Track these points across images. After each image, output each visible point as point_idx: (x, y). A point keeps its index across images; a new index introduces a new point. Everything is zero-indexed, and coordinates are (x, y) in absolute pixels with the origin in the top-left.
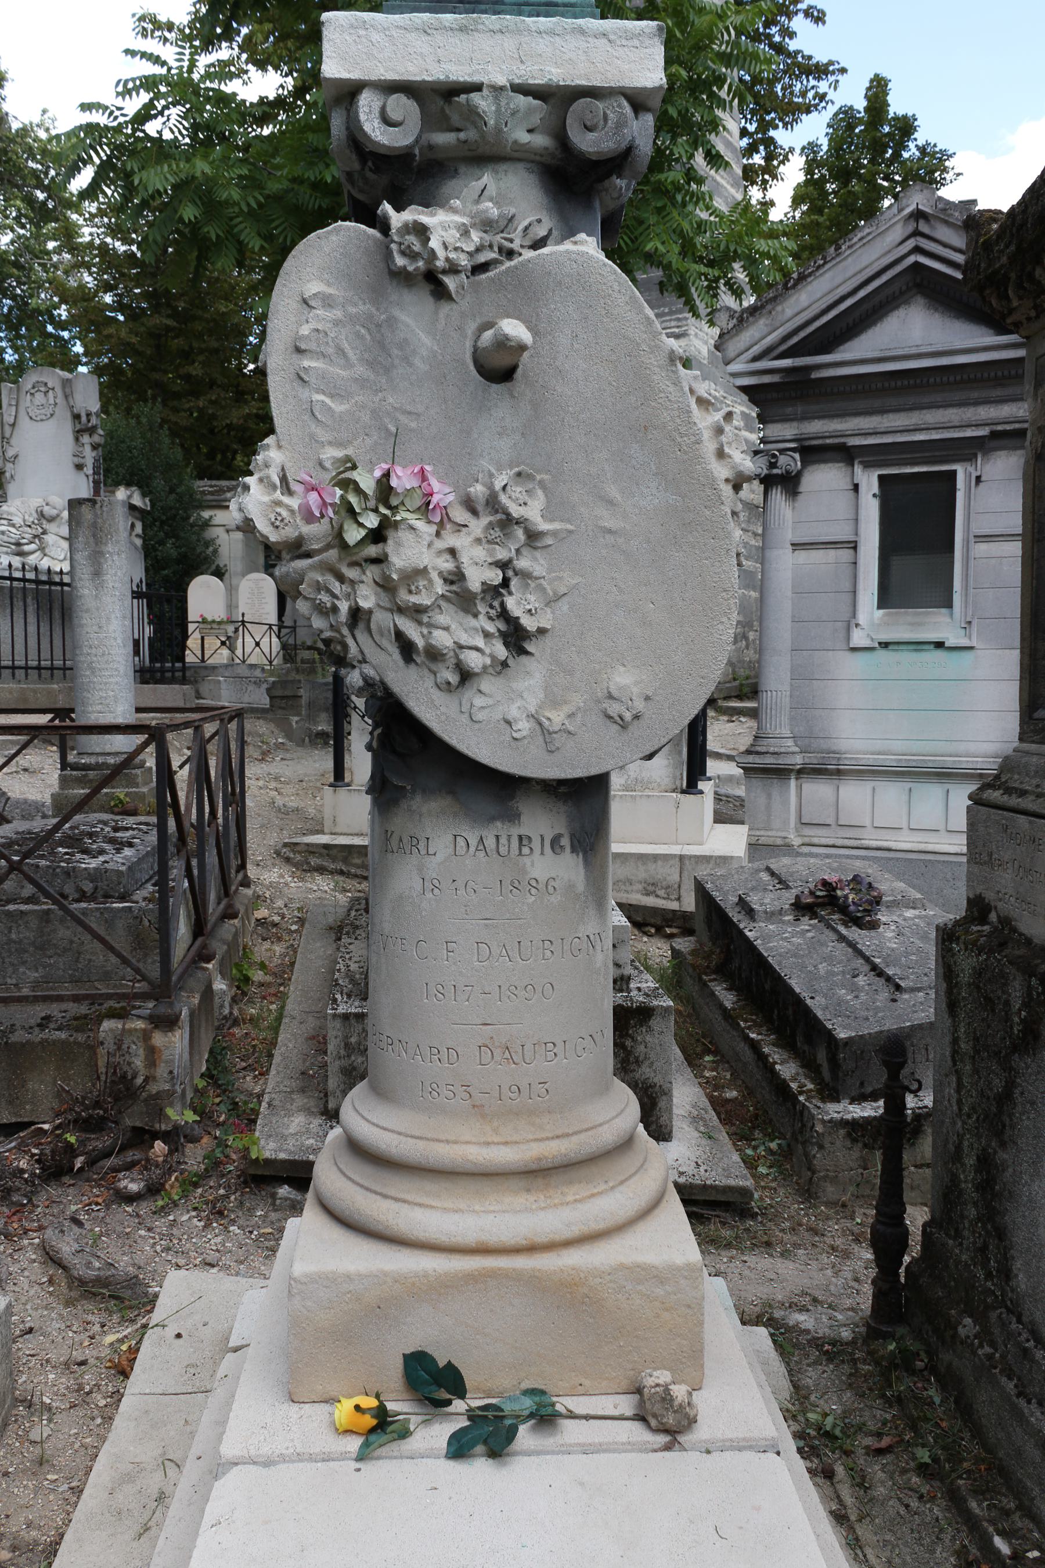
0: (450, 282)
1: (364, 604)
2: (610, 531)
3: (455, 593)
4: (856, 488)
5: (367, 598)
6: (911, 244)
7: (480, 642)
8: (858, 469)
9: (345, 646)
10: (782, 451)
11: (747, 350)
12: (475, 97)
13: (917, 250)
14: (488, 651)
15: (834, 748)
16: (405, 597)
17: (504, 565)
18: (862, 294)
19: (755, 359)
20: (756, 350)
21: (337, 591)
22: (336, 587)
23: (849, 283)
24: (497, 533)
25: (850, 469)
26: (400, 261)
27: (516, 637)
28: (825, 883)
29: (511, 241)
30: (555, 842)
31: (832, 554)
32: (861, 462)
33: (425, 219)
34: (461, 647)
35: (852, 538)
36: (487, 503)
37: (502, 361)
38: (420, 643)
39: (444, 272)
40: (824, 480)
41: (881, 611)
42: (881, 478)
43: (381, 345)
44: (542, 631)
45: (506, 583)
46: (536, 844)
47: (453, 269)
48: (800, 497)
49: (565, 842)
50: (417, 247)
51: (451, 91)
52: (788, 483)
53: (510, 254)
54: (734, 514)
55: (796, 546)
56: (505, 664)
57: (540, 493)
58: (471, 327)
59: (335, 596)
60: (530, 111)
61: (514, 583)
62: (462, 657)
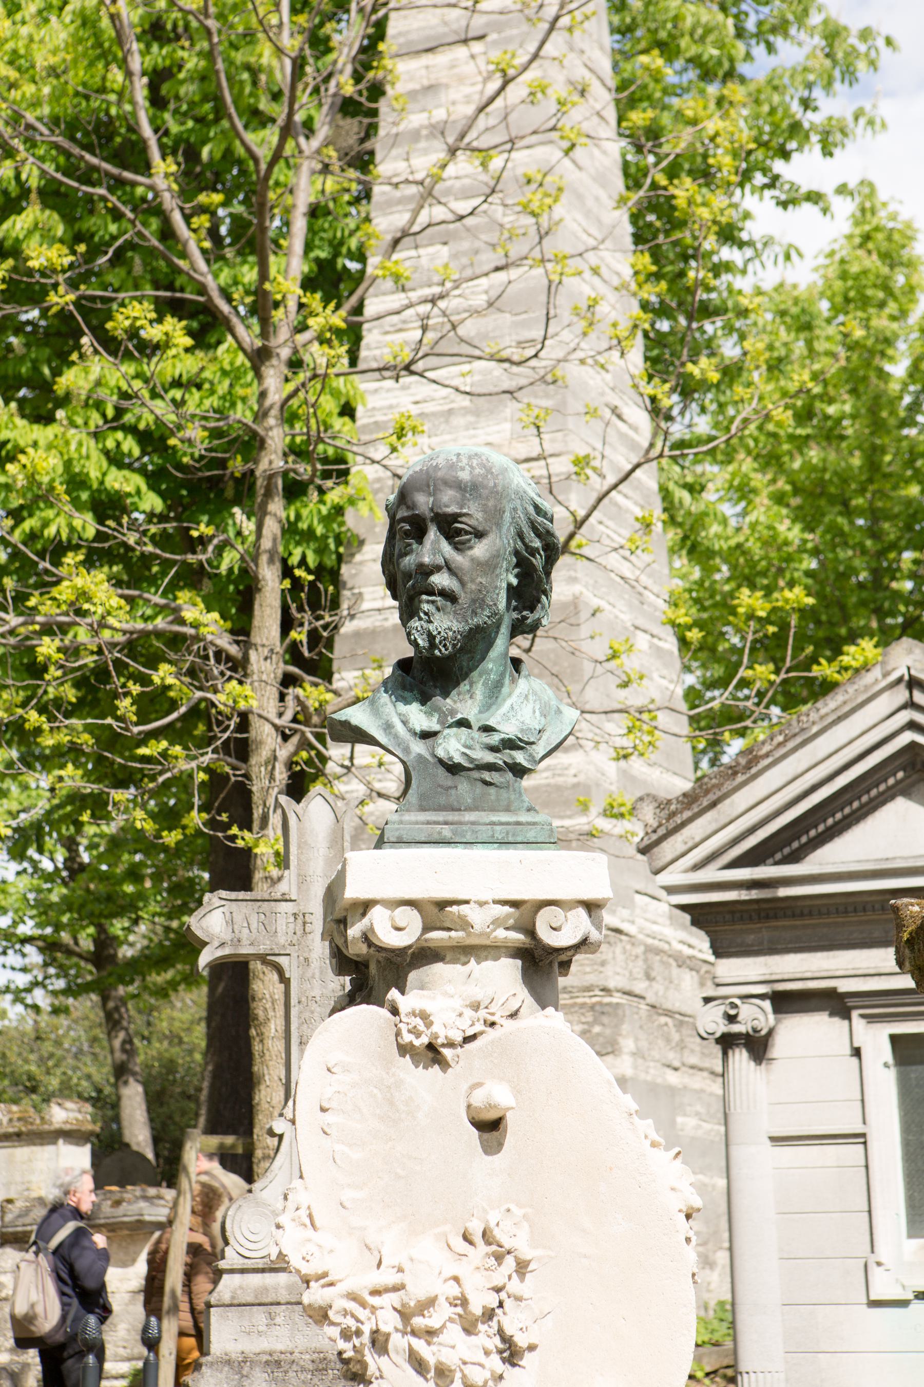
0: (447, 1052)
1: (384, 1328)
2: (585, 1256)
3: (460, 1316)
4: (857, 1052)
5: (389, 1322)
6: (905, 716)
7: (481, 1358)
8: (858, 1023)
9: (365, 1366)
11: (683, 855)
12: (464, 909)
13: (912, 726)
14: (487, 1366)
16: (418, 1322)
17: (498, 1290)
19: (697, 867)
21: (362, 1318)
22: (362, 1314)
24: (492, 1261)
25: (846, 1022)
26: (407, 1038)
27: (511, 1353)
29: (493, 1014)
32: (863, 1016)
33: (429, 1007)
34: (465, 1363)
35: (858, 1128)
36: (484, 1234)
37: (492, 1115)
38: (432, 1361)
39: (443, 1045)
43: (391, 1103)
44: (532, 1348)
45: (501, 1305)
47: (451, 1045)
50: (422, 1027)
51: (442, 905)
52: (758, 1046)
53: (493, 1024)
54: (688, 1240)
55: (776, 1140)
56: (501, 1377)
57: (526, 1225)
58: (465, 1087)
59: (358, 1320)
60: (508, 916)
61: (508, 1303)
62: (466, 1372)
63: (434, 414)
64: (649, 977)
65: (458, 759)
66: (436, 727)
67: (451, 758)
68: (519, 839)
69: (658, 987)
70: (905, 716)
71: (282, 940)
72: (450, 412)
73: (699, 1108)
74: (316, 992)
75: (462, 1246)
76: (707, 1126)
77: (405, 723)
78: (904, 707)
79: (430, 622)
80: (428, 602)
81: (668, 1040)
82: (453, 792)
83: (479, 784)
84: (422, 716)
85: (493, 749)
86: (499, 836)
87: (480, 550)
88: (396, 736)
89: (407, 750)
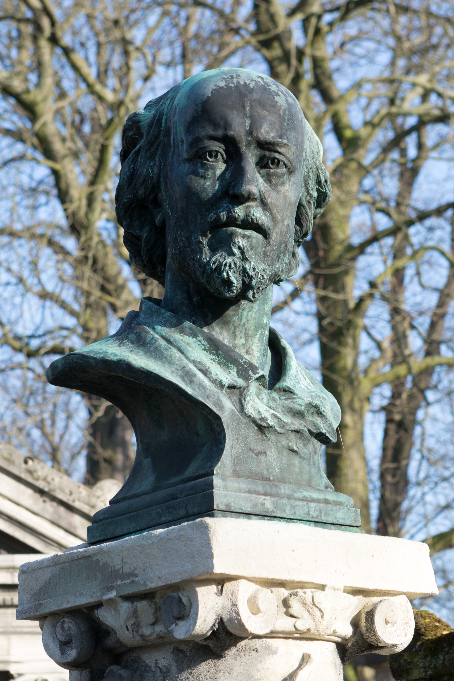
67: (263, 419)
68: (331, 520)
79: (244, 259)
80: (244, 237)
82: (262, 458)
83: (286, 452)
85: (299, 414)
86: (314, 514)
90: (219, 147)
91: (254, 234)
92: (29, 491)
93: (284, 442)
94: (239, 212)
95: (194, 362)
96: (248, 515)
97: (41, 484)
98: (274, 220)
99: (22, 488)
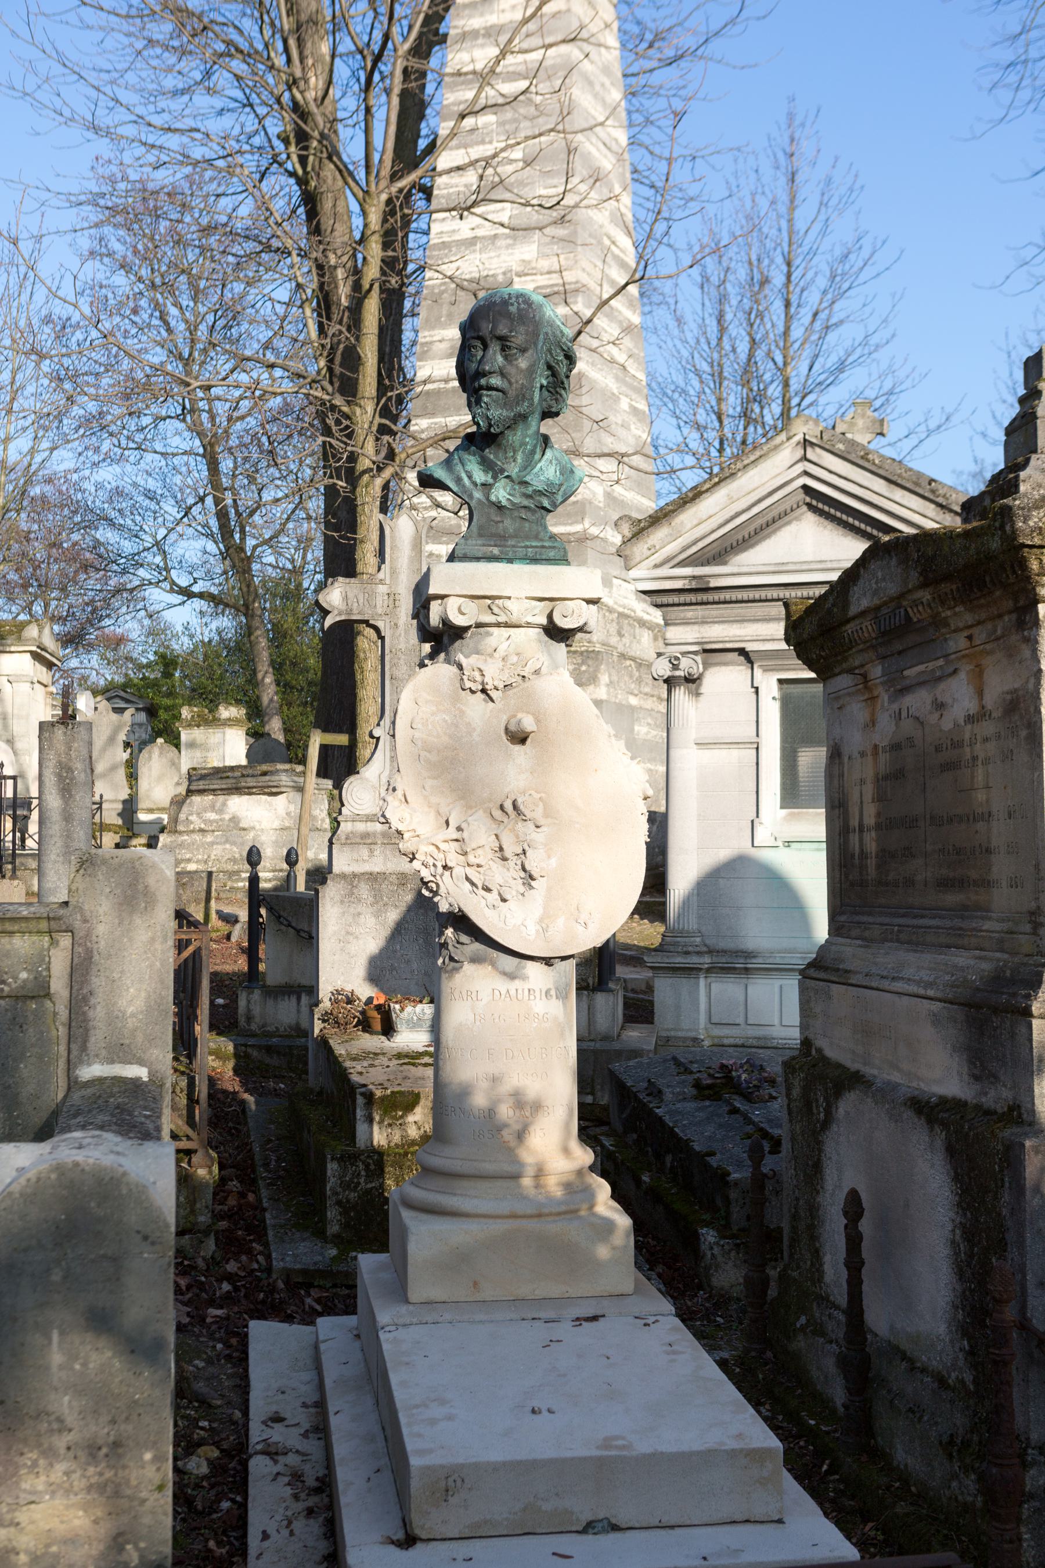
0: (493, 694)
6: (799, 468)
10: (684, 654)
12: (507, 603)
13: (806, 473)
15: (742, 947)
16: (472, 859)
18: (755, 510)
19: (656, 566)
20: (658, 558)
23: (744, 500)
28: (723, 1067)
30: (547, 992)
31: (735, 753)
40: (726, 680)
41: (785, 811)
42: (781, 681)
46: (537, 994)
48: (701, 698)
49: (553, 992)
57: (541, 804)
63: (484, 238)
64: (620, 635)
65: (504, 503)
66: (491, 481)
69: (626, 640)
70: (799, 468)
71: (380, 611)
72: (495, 236)
73: (650, 721)
74: (402, 646)
75: (498, 814)
76: (654, 733)
77: (470, 477)
78: (800, 460)
81: (631, 677)
84: (481, 473)
87: (523, 363)
88: (464, 486)
89: (471, 496)
90: (479, 344)
91: (494, 393)
92: (933, 506)
93: (516, 514)
94: (483, 382)
95: (466, 472)
96: (478, 559)
97: (940, 500)
98: (510, 383)
99: (927, 503)
